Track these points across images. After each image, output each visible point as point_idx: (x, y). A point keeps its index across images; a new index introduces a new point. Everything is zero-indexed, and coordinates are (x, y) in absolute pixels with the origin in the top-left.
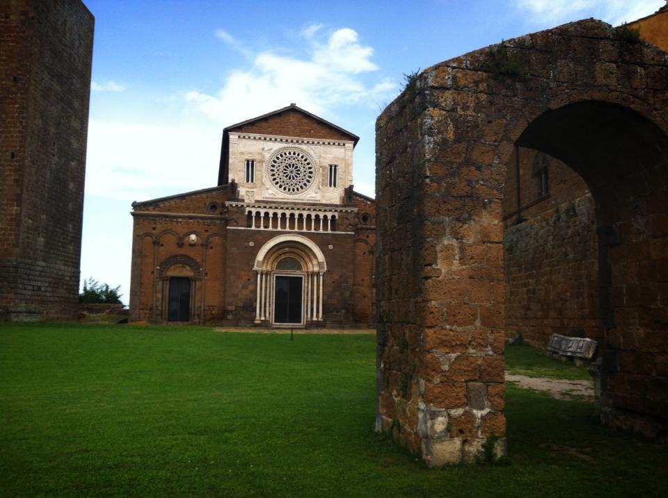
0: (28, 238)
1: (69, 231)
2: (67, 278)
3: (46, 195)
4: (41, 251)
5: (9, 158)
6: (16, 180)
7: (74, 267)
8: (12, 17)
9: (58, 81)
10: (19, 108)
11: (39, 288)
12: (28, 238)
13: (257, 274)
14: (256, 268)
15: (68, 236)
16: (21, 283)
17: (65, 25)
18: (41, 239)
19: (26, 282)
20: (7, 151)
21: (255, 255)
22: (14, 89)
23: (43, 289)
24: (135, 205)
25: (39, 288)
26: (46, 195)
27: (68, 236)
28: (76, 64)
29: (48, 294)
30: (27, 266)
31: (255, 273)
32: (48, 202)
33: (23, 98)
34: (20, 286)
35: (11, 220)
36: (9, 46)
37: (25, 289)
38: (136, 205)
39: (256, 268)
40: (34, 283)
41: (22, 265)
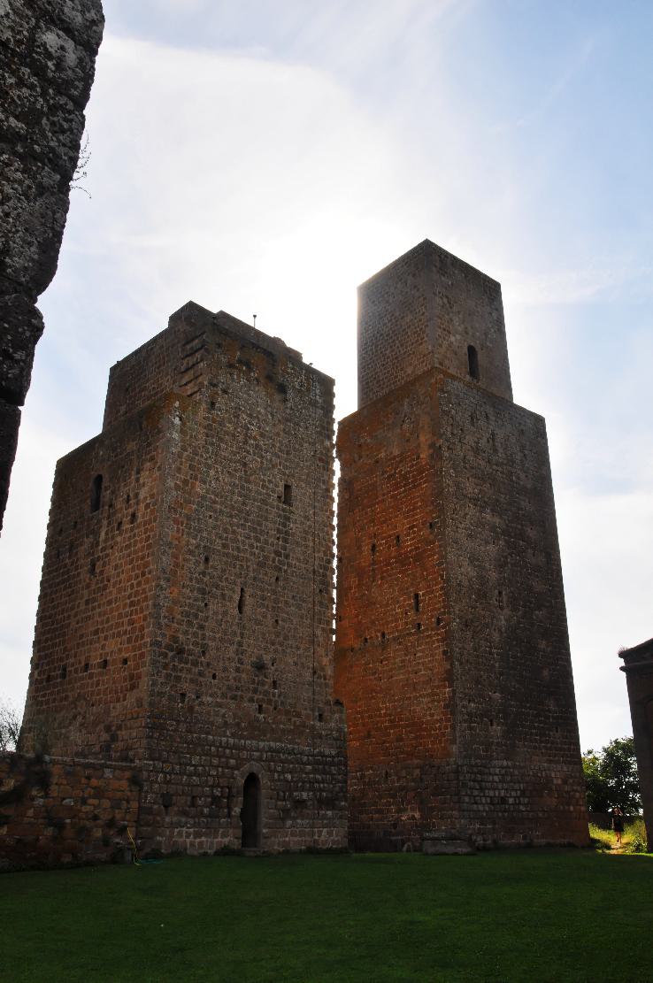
0: (471, 728)
1: (549, 711)
2: (560, 782)
3: (497, 665)
5: (434, 625)
6: (445, 653)
7: (575, 763)
8: (422, 456)
9: (492, 510)
10: (438, 559)
11: (503, 800)
15: (548, 717)
16: (466, 795)
17: (493, 440)
18: (497, 730)
19: (476, 793)
20: (432, 616)
22: (431, 537)
23: (511, 801)
24: (623, 654)
25: (503, 800)
26: (497, 665)
27: (548, 717)
28: (521, 483)
29: (522, 808)
30: (475, 770)
32: (501, 674)
33: (440, 546)
34: (467, 799)
35: (446, 706)
36: (422, 489)
38: (623, 654)
40: (492, 793)
41: (465, 768)
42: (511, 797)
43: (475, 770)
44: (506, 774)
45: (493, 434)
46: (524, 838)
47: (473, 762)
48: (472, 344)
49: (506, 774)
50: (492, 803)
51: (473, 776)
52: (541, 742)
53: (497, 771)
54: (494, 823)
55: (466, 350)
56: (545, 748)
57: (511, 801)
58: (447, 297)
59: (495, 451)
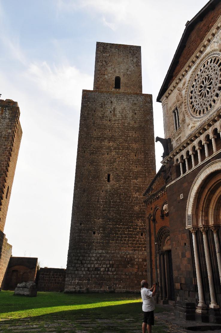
2: (141, 260)
4: (97, 243)
12: (79, 236)
13: (191, 233)
14: (189, 226)
17: (114, 111)
21: (184, 209)
23: (102, 269)
25: (97, 269)
29: (109, 273)
31: (188, 233)
37: (77, 270)
39: (189, 226)
40: (89, 266)
42: (102, 267)
43: (79, 255)
44: (101, 256)
45: (114, 109)
46: (109, 288)
47: (78, 251)
48: (118, 76)
49: (101, 256)
50: (88, 270)
51: (77, 258)
52: (128, 240)
53: (94, 255)
54: (89, 280)
55: (114, 79)
56: (133, 244)
57: (102, 269)
58: (105, 61)
59: (115, 115)
